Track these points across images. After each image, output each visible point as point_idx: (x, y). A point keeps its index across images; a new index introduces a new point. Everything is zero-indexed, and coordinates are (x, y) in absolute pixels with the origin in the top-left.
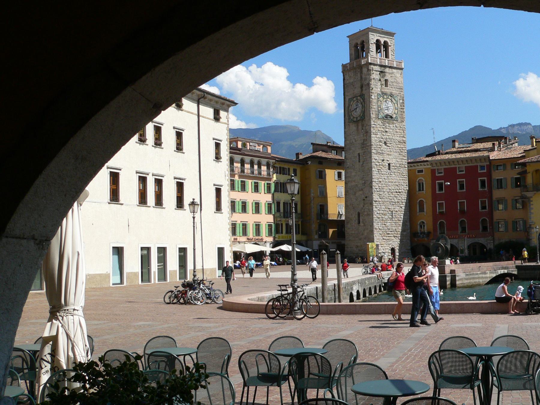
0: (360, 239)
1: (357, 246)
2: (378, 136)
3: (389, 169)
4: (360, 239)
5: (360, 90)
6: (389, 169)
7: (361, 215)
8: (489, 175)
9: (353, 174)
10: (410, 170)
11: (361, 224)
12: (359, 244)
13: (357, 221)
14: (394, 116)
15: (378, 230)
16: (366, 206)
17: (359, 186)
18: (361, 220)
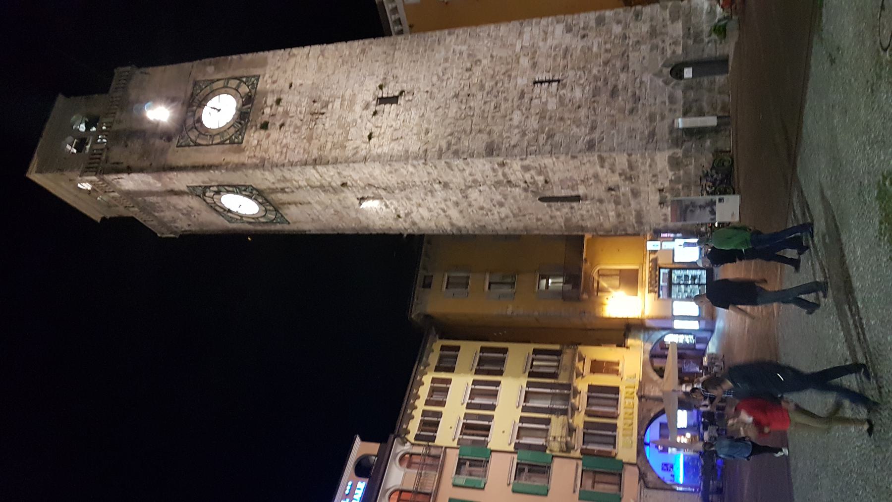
0: (635, 194)
2: (292, 146)
3: (393, 100)
4: (635, 194)
5: (186, 198)
6: (393, 100)
7: (548, 194)
10: (411, 26)
11: (581, 191)
12: (656, 198)
13: (575, 204)
14: (244, 89)
15: (596, 135)
16: (512, 178)
17: (454, 199)
18: (563, 193)
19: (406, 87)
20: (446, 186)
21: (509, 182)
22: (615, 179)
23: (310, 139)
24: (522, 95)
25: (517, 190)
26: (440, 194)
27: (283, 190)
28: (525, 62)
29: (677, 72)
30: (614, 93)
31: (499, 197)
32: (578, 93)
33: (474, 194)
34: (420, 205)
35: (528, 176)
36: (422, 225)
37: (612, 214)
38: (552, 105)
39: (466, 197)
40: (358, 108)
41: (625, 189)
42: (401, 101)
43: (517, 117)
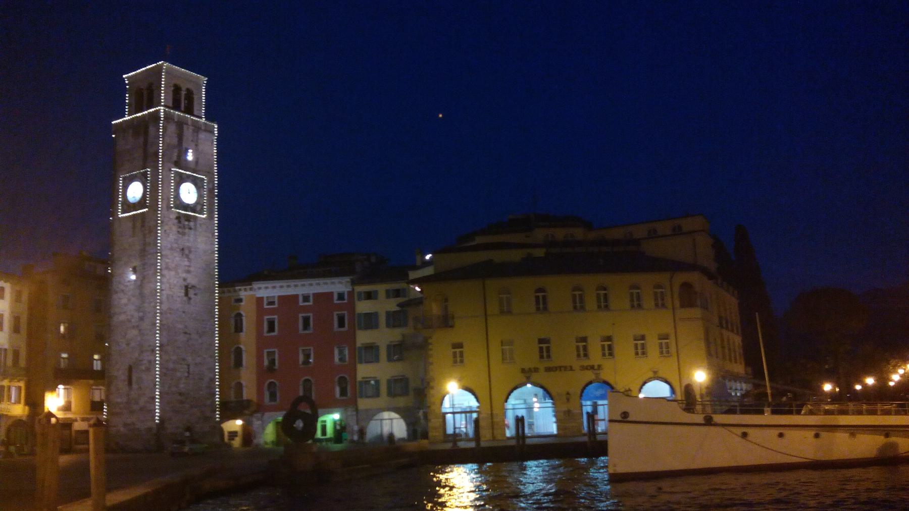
1: (126, 425)
3: (187, 294)
8: (351, 307)
9: (124, 301)
11: (135, 386)
12: (129, 421)
18: (134, 379)
19: (192, 301)
20: (141, 319)
21: (142, 352)
22: (142, 402)
23: (171, 249)
24: (184, 360)
25: (136, 355)
26: (136, 315)
27: (143, 226)
28: (198, 360)
29: (188, 429)
30: (182, 402)
31: (133, 344)
32: (182, 386)
33: (135, 332)
34: (129, 300)
35: (145, 362)
36: (115, 296)
37: (119, 400)
38: (179, 374)
39: (134, 327)
40: (184, 275)
41: (135, 407)
42: (185, 298)
43: (174, 358)
